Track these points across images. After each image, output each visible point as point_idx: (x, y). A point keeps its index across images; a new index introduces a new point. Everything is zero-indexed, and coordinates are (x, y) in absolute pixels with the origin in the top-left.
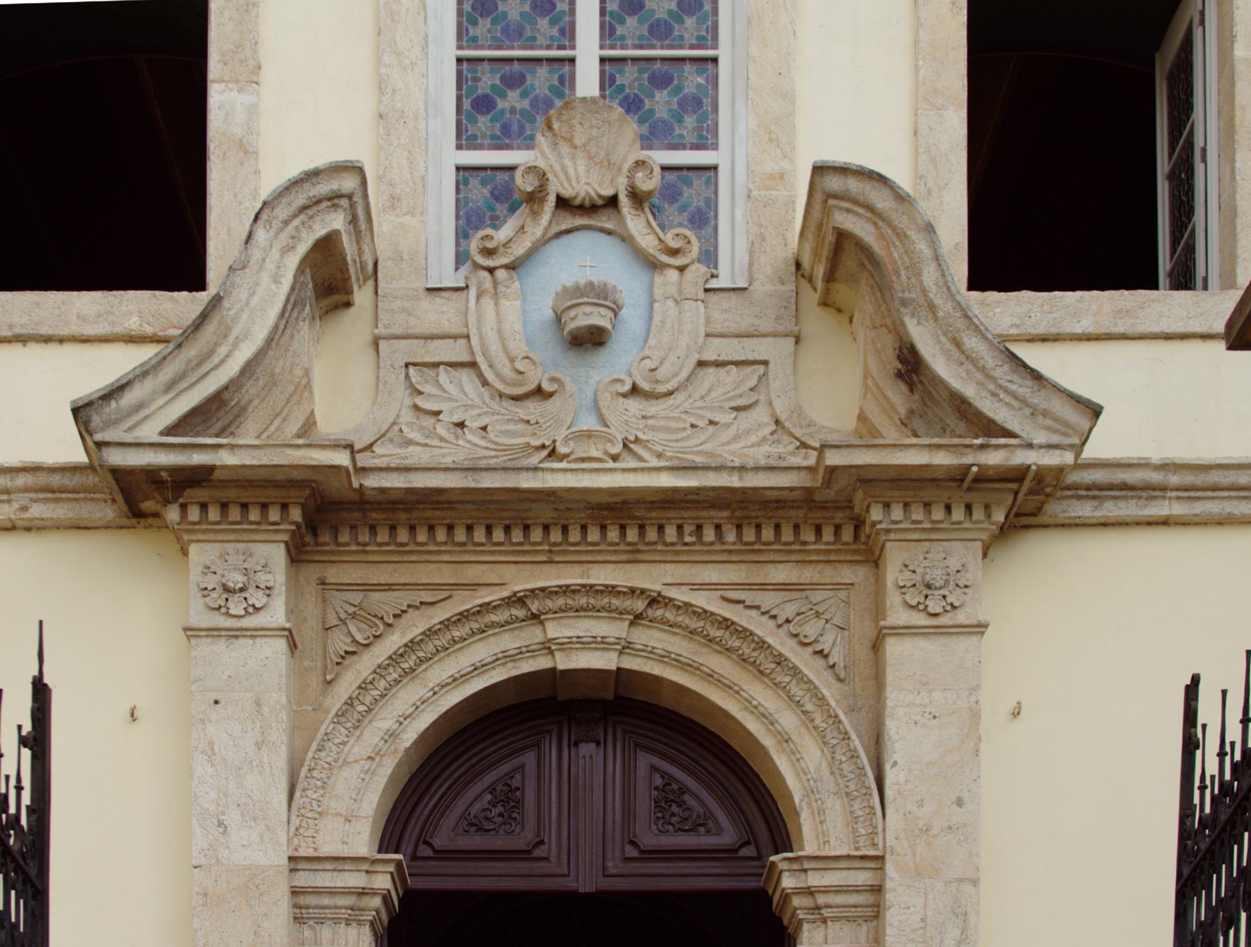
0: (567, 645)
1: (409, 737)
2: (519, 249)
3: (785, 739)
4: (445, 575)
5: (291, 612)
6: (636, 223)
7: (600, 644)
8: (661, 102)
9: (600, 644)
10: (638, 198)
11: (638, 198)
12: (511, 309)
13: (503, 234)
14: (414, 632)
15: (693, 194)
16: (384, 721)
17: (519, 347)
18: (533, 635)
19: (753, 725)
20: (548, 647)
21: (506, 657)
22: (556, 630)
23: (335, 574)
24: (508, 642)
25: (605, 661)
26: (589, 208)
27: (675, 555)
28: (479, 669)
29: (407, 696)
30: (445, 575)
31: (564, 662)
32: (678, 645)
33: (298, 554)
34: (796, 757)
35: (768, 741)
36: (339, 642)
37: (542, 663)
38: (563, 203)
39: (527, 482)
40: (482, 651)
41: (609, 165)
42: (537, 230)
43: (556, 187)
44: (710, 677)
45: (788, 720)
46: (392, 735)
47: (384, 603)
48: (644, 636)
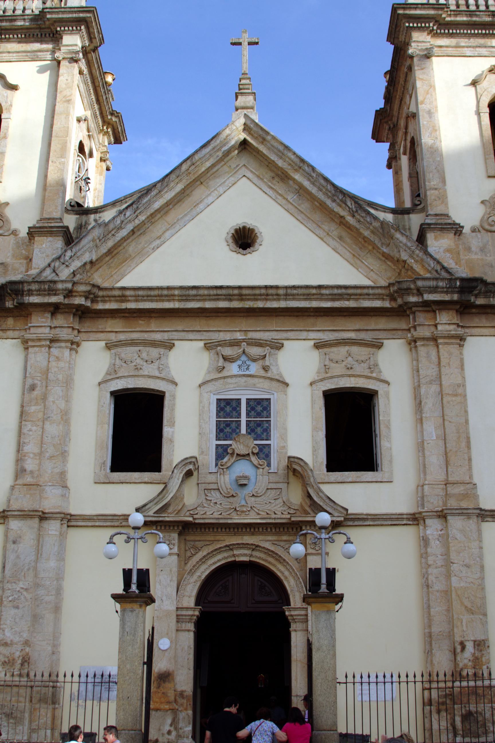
0: (238, 556)
1: (203, 577)
2: (229, 464)
3: (286, 578)
4: (212, 538)
5: (179, 549)
6: (254, 459)
7: (245, 555)
8: (259, 430)
9: (245, 555)
10: (253, 453)
11: (253, 453)
12: (227, 477)
13: (225, 460)
14: (205, 553)
15: (266, 450)
16: (198, 574)
17: (229, 486)
18: (231, 553)
19: (279, 574)
20: (234, 556)
21: (225, 558)
22: (236, 552)
23: (188, 538)
24: (225, 554)
25: (246, 559)
26: (244, 456)
27: (261, 537)
28: (219, 561)
29: (203, 567)
30: (212, 538)
31: (238, 559)
32: (262, 555)
33: (180, 534)
34: (288, 582)
35: (282, 578)
36: (189, 554)
37: (233, 559)
38: (238, 455)
39: (230, 521)
40: (219, 557)
41: (247, 446)
42: (232, 460)
43: (236, 451)
44: (270, 563)
45: (287, 573)
46: (200, 576)
47: (199, 544)
48: (255, 553)
